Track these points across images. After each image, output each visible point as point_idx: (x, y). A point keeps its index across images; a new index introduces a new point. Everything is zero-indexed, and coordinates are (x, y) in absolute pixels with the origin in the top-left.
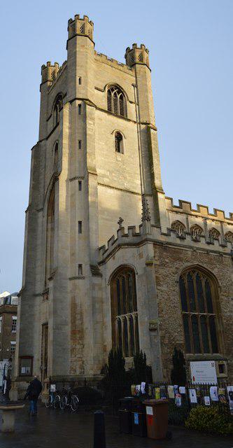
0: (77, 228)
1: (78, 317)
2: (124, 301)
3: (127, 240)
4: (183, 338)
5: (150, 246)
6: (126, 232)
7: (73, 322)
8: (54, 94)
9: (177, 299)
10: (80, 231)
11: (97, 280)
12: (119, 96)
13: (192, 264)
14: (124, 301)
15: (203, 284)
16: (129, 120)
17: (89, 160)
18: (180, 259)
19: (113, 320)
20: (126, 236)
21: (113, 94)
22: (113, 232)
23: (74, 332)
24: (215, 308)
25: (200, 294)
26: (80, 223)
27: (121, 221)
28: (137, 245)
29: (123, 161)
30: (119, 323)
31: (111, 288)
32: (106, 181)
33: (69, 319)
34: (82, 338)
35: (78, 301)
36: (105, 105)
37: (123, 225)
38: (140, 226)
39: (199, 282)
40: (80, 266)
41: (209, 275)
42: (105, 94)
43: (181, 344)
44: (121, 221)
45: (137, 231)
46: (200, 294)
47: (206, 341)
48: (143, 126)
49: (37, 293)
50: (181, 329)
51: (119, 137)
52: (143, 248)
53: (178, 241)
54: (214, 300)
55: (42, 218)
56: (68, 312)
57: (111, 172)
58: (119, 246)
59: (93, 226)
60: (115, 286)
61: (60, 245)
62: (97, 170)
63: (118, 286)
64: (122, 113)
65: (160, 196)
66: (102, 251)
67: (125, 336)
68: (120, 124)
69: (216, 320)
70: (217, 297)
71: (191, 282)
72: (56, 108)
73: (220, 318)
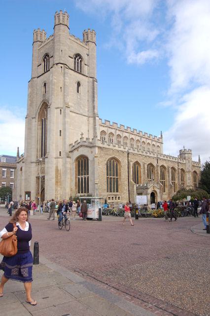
0: (59, 134)
1: (59, 175)
2: (82, 171)
3: (86, 144)
4: (106, 187)
5: (97, 149)
6: (85, 140)
7: (57, 177)
8: (43, 52)
9: (105, 171)
10: (60, 135)
11: (68, 160)
12: (80, 60)
13: (111, 157)
14: (82, 171)
15: (115, 165)
16: (84, 75)
17: (66, 99)
18: (107, 154)
19: (76, 178)
20: (85, 142)
21: (77, 59)
22: (78, 138)
23: (57, 182)
24: (119, 175)
25: (113, 168)
26: (60, 131)
27: (82, 134)
28: (91, 147)
29: (80, 99)
30: (79, 179)
31: (76, 164)
32: (72, 109)
33: (54, 176)
34: (61, 185)
35: (59, 169)
36: (72, 66)
37: (83, 136)
38: (93, 139)
39: (114, 165)
40: (60, 152)
41: (117, 161)
42: (73, 60)
43: (105, 189)
44: (83, 134)
45: (91, 141)
46: (113, 168)
47: (114, 187)
48: (91, 79)
49: (32, 161)
50: (106, 183)
51: (79, 84)
52: (93, 149)
53: (107, 147)
54: (118, 171)
55: (36, 124)
56: (54, 173)
57: (75, 104)
58: (81, 146)
59: (67, 134)
60: (77, 163)
61: (51, 142)
62: (70, 104)
63: (79, 162)
64: (81, 71)
65: (97, 118)
66: (71, 146)
67: (83, 185)
68: (79, 77)
69: (119, 180)
70: (120, 170)
71: (110, 164)
72: (44, 60)
73: (120, 178)
